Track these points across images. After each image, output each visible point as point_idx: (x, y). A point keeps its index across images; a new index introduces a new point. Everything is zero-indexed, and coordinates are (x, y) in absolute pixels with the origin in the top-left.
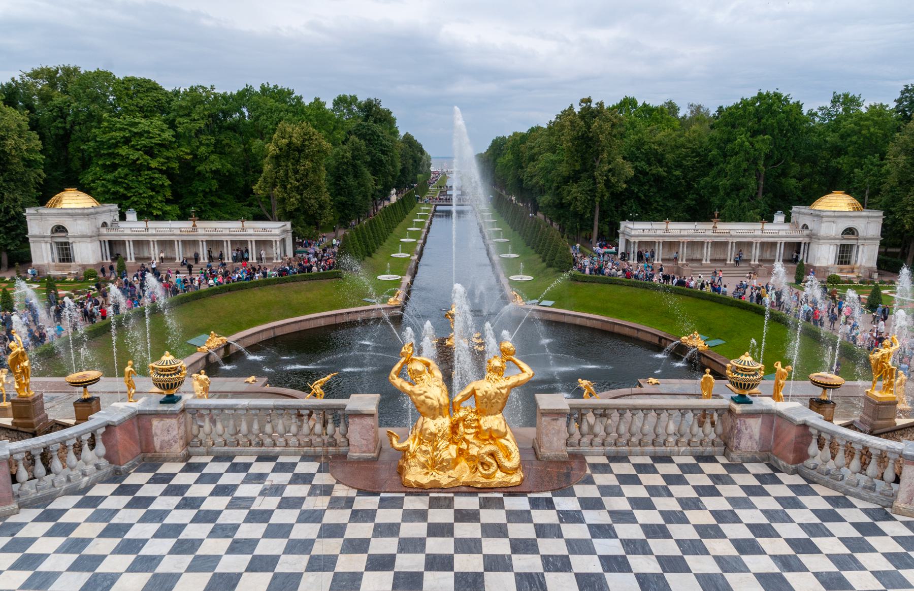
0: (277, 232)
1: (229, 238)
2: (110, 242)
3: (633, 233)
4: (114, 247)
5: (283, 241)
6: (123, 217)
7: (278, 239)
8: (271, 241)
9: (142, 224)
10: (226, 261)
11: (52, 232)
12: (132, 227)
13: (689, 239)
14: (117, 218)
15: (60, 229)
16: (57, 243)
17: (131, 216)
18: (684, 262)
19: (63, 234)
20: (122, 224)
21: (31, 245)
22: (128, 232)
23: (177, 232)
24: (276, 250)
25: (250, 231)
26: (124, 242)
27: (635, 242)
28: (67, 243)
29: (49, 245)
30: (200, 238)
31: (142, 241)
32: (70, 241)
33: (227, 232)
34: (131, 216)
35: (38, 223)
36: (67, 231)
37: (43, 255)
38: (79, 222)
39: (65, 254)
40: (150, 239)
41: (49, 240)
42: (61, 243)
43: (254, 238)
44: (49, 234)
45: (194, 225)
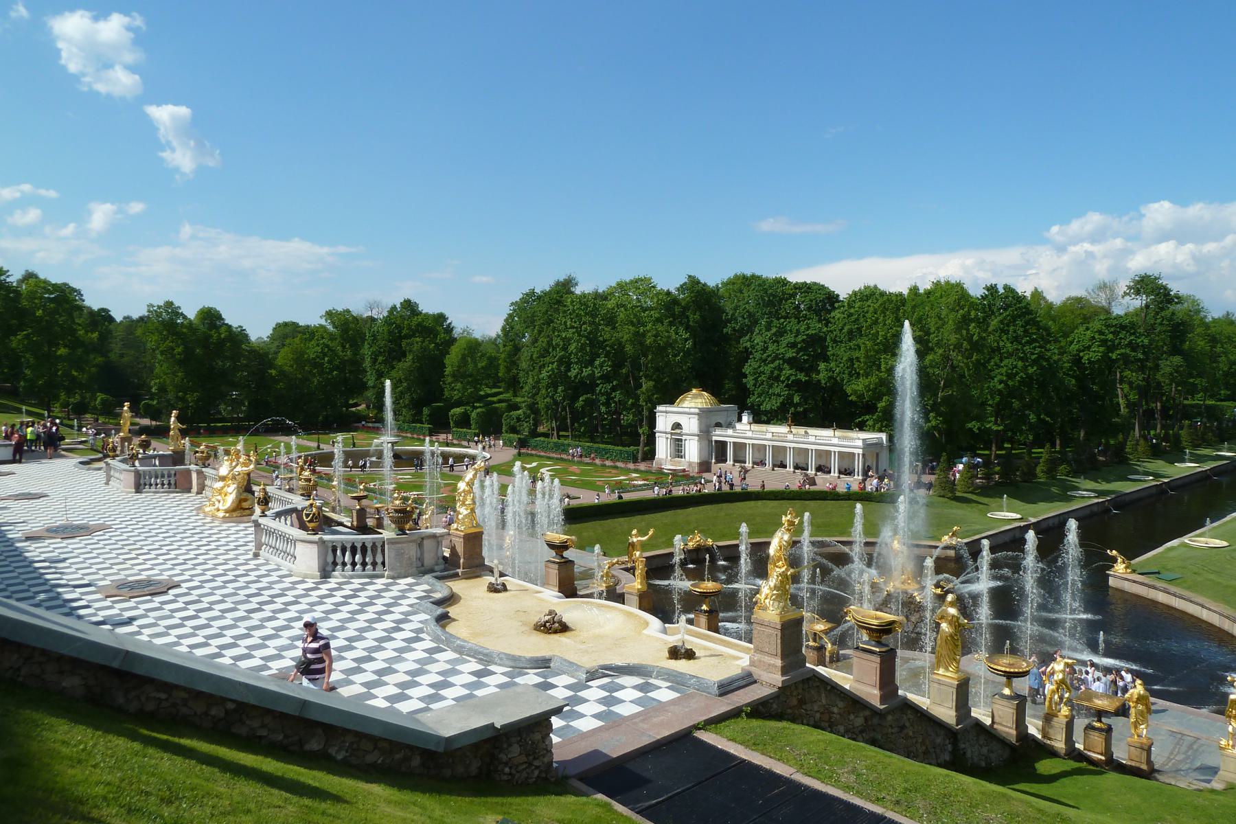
0: (860, 443)
4: (720, 450)
6: (740, 420)
7: (860, 451)
9: (748, 427)
12: (745, 431)
15: (677, 426)
19: (678, 431)
20: (738, 426)
23: (769, 436)
24: (858, 465)
25: (835, 441)
34: (745, 418)
35: (665, 418)
37: (663, 447)
39: (678, 449)
43: (837, 449)
44: (669, 429)
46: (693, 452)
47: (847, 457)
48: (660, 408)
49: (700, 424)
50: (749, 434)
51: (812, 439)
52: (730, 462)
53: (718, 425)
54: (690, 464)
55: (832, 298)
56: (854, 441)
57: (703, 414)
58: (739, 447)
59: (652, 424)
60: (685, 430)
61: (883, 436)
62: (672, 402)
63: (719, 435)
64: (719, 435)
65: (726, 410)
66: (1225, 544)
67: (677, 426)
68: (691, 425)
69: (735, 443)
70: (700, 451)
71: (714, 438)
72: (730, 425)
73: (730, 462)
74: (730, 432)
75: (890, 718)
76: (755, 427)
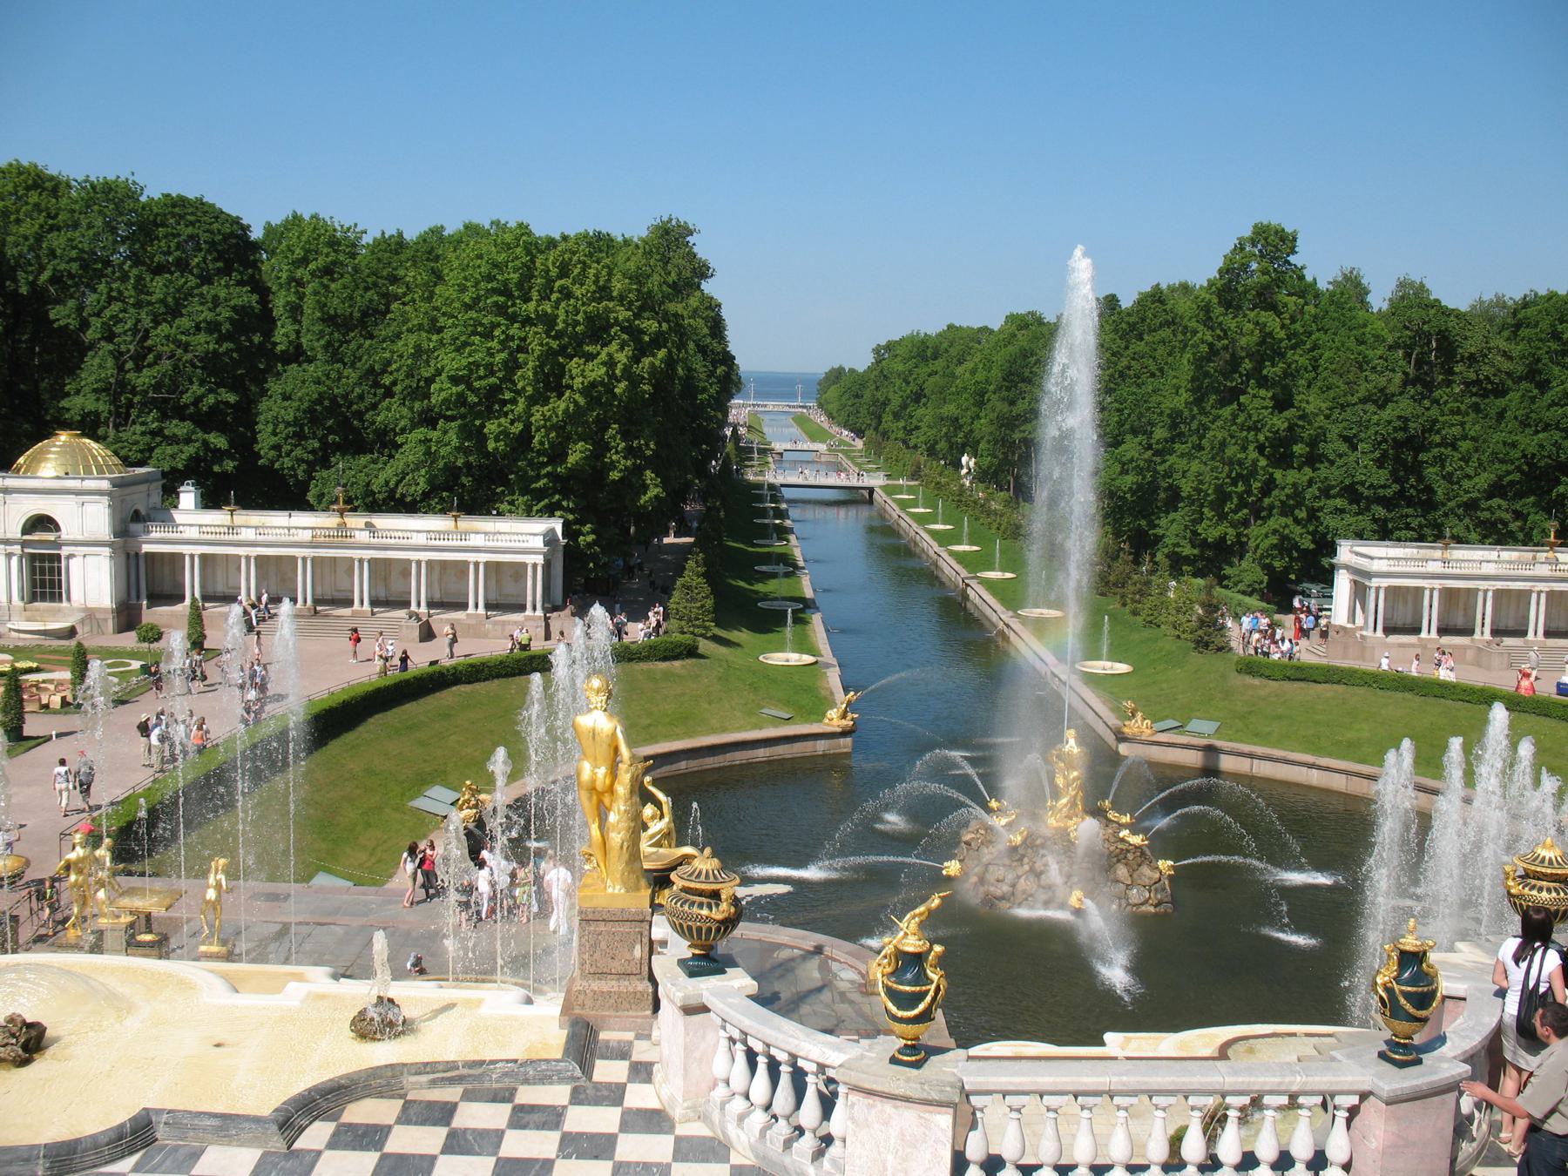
0: (538, 543)
1: (424, 556)
3: (1376, 566)
5: (547, 566)
7: (540, 559)
8: (524, 565)
11: (23, 533)
12: (192, 524)
13: (1500, 585)
14: (156, 498)
15: (41, 523)
16: (33, 557)
17: (188, 497)
18: (1487, 636)
19: (51, 537)
22: (193, 533)
23: (306, 536)
24: (534, 588)
25: (476, 541)
26: (182, 556)
27: (1378, 589)
29: (15, 560)
30: (356, 554)
31: (213, 556)
32: (65, 551)
33: (421, 539)
34: (188, 497)
36: (57, 528)
38: (89, 508)
41: (17, 549)
42: (42, 557)
43: (483, 558)
44: (15, 532)
45: (342, 526)
46: (92, 582)
53: (137, 517)
54: (90, 615)
55: (238, 230)
60: (70, 529)
66: (1123, 668)
68: (86, 518)
69: (205, 558)
70: (116, 577)
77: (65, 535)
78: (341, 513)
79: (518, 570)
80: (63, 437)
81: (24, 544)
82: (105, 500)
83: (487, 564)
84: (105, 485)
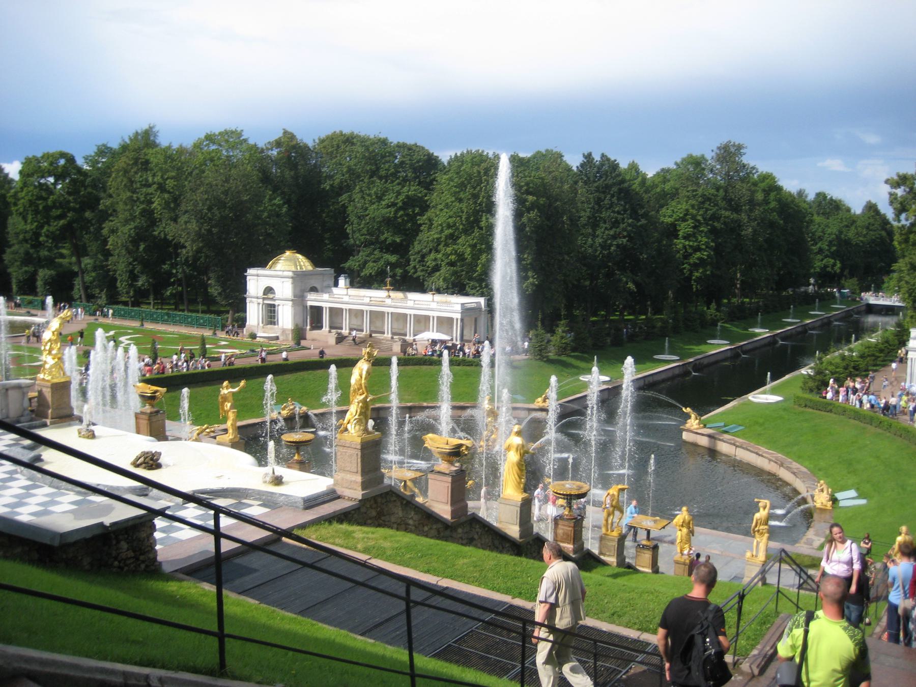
0: (458, 308)
2: (311, 307)
4: (316, 314)
6: (336, 284)
7: (459, 316)
8: (451, 319)
9: (345, 292)
10: (407, 338)
14: (332, 283)
15: (269, 290)
19: (271, 296)
20: (335, 290)
21: (248, 305)
23: (367, 300)
28: (274, 306)
32: (276, 303)
34: (342, 281)
37: (254, 314)
39: (271, 315)
40: (343, 306)
41: (261, 301)
43: (436, 314)
44: (261, 294)
46: (286, 318)
47: (445, 323)
48: (251, 271)
49: (295, 288)
50: (346, 299)
51: (410, 304)
52: (326, 328)
53: (314, 289)
54: (284, 331)
56: (452, 305)
57: (299, 278)
58: (336, 313)
59: (243, 288)
60: (278, 294)
61: (482, 301)
62: (263, 264)
63: (313, 300)
64: (313, 300)
65: (322, 274)
67: (269, 290)
68: (284, 289)
69: (331, 309)
71: (309, 303)
72: (326, 289)
73: (326, 328)
74: (326, 296)
75: (460, 530)
76: (354, 292)
77: (277, 296)
78: (388, 290)
79: (450, 320)
80: (288, 253)
81: (264, 299)
82: (290, 280)
83: (438, 317)
84: (291, 274)
